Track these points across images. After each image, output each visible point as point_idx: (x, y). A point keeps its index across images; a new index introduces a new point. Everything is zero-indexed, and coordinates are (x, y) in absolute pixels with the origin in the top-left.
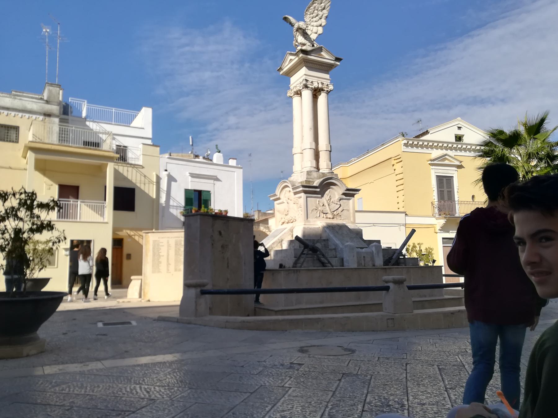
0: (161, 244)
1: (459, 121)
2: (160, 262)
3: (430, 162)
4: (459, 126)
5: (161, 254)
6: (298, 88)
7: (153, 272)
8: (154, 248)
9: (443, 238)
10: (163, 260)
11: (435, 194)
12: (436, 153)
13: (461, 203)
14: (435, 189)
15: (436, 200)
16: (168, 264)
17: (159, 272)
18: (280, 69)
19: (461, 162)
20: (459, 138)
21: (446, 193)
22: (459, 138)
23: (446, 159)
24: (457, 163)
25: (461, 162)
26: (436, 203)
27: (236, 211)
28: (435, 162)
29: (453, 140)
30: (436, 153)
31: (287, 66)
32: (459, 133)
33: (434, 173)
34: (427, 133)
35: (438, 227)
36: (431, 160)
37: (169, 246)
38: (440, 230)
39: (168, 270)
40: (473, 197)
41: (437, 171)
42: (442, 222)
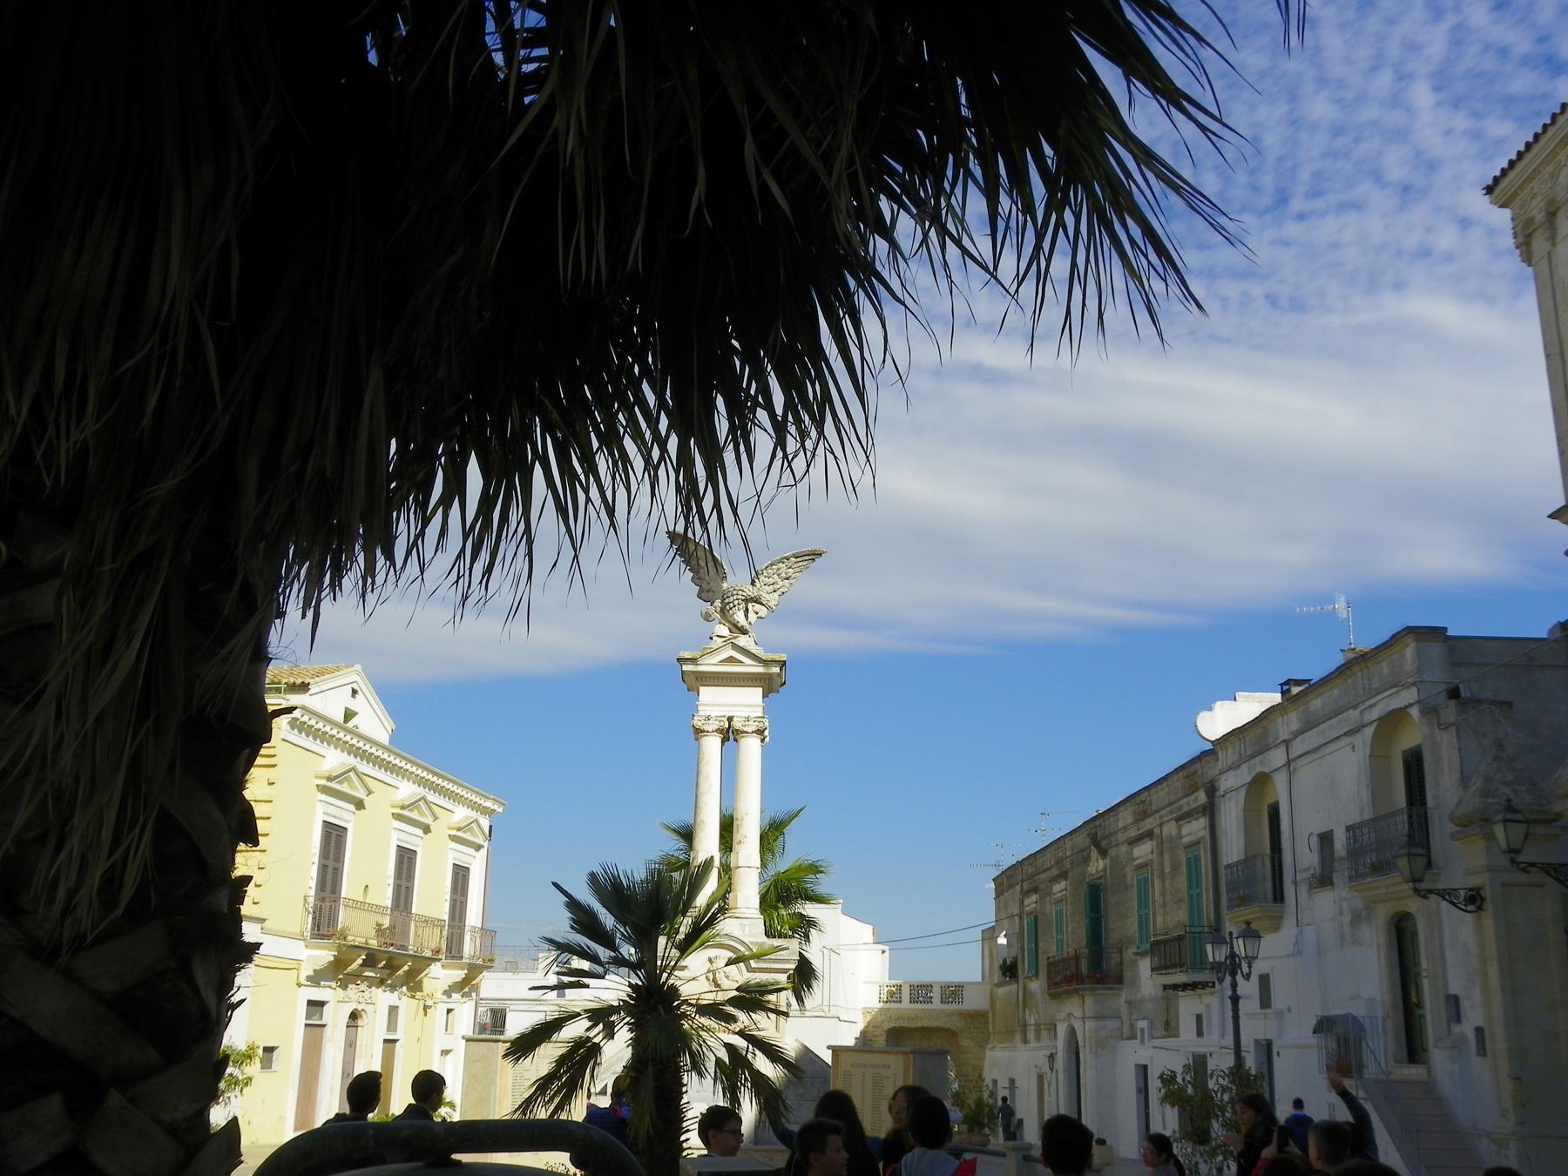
1: (354, 675)
3: (323, 782)
6: (737, 724)
9: (311, 1003)
11: (314, 871)
12: (335, 760)
14: (316, 859)
15: (312, 892)
18: (693, 661)
19: (370, 793)
20: (349, 715)
21: (330, 871)
22: (349, 715)
23: (348, 779)
24: (361, 794)
25: (370, 793)
26: (311, 900)
27: (1325, 1107)
28: (332, 785)
29: (341, 719)
30: (335, 760)
31: (710, 665)
32: (354, 705)
33: (323, 810)
34: (304, 687)
35: (307, 971)
36: (330, 779)
38: (309, 978)
41: (331, 809)
42: (324, 955)
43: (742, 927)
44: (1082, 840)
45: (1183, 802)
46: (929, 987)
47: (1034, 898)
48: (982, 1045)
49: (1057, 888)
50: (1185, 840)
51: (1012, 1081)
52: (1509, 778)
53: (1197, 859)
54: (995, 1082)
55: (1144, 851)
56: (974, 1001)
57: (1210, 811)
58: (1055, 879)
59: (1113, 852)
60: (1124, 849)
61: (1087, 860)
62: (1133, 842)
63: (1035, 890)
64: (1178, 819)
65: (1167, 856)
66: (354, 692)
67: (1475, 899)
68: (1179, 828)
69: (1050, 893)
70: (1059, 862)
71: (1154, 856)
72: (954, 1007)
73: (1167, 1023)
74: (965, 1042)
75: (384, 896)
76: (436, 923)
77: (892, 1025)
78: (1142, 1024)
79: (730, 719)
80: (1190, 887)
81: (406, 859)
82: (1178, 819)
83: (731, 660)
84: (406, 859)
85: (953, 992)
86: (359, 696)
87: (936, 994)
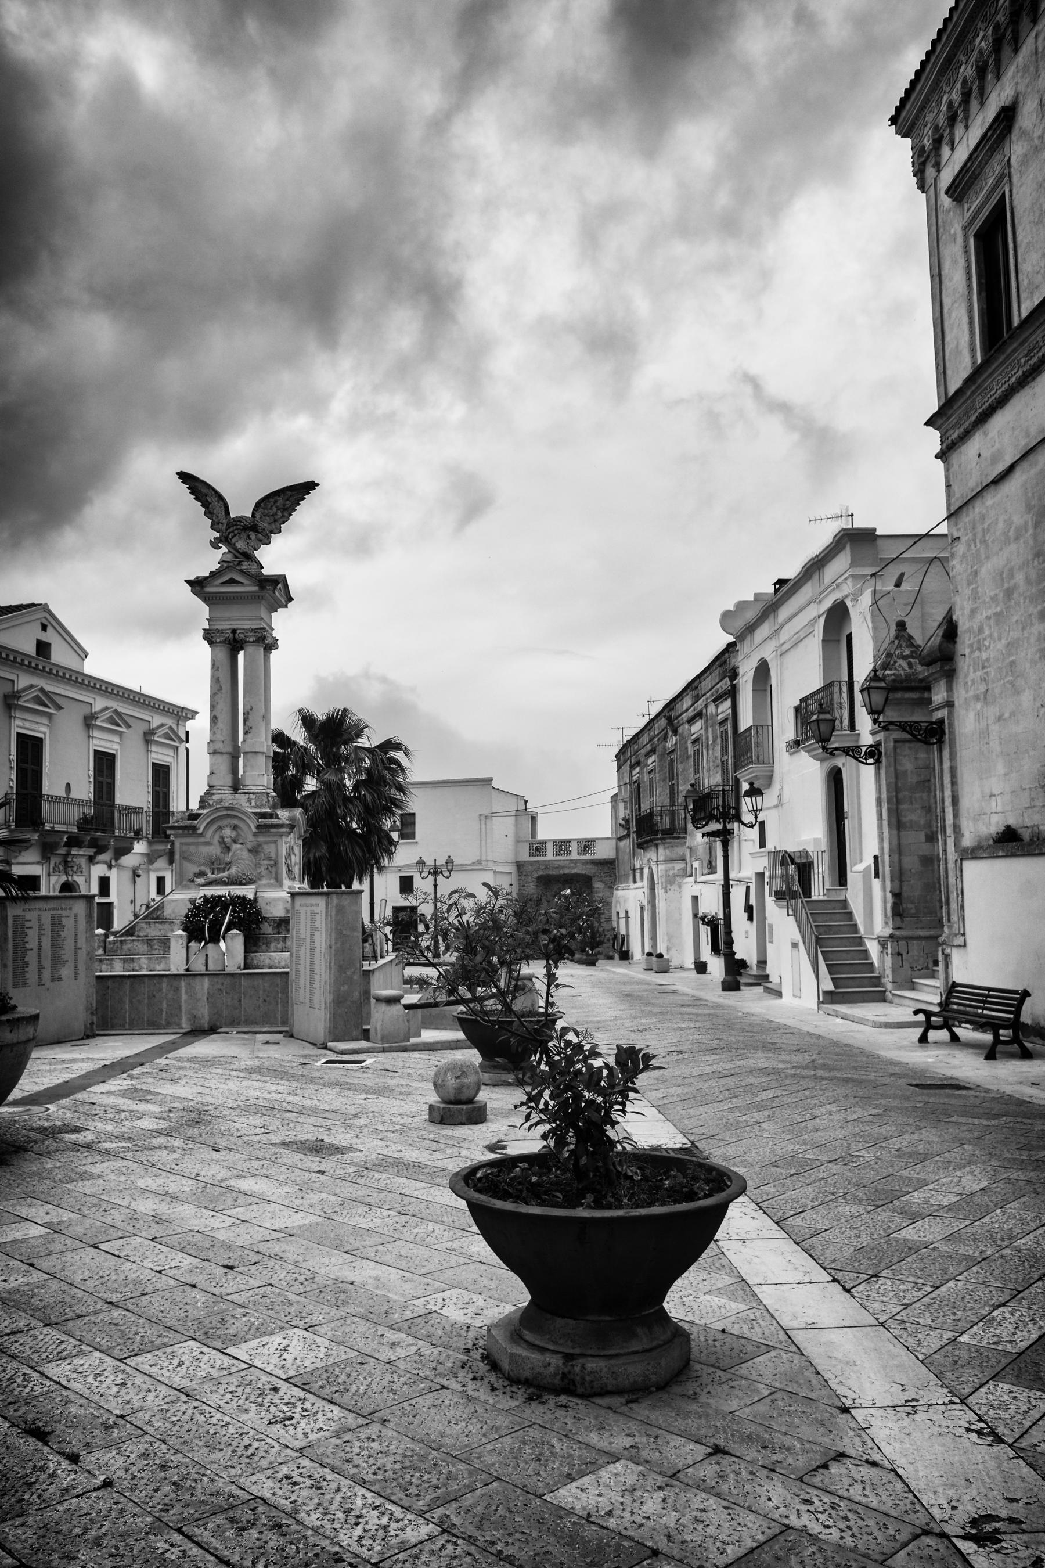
0: (28, 924)
2: (27, 964)
4: (45, 622)
5: (28, 946)
6: (240, 636)
7: (15, 986)
8: (15, 933)
10: (31, 958)
13: (54, 799)
16: (41, 968)
17: (25, 984)
20: (43, 648)
32: (44, 637)
37: (41, 928)
39: (40, 979)
40: (68, 785)
43: (249, 800)
44: (663, 722)
45: (718, 686)
46: (567, 842)
47: (637, 770)
48: (611, 887)
49: (650, 760)
50: (720, 717)
51: (627, 912)
52: (907, 652)
53: (726, 731)
54: (618, 913)
55: (697, 727)
56: (604, 852)
57: (732, 693)
58: (648, 755)
59: (680, 730)
60: (686, 726)
61: (666, 736)
62: (691, 721)
63: (638, 763)
64: (714, 701)
65: (710, 730)
66: (44, 628)
67: (874, 753)
68: (717, 706)
69: (647, 765)
70: (651, 740)
71: (703, 732)
72: (588, 857)
73: (710, 863)
74: (597, 885)
75: (84, 790)
76: (137, 810)
77: (541, 873)
78: (696, 864)
79: (234, 631)
80: (722, 755)
81: (105, 763)
82: (714, 701)
83: (231, 582)
84: (105, 763)
85: (586, 845)
86: (49, 629)
87: (574, 848)
